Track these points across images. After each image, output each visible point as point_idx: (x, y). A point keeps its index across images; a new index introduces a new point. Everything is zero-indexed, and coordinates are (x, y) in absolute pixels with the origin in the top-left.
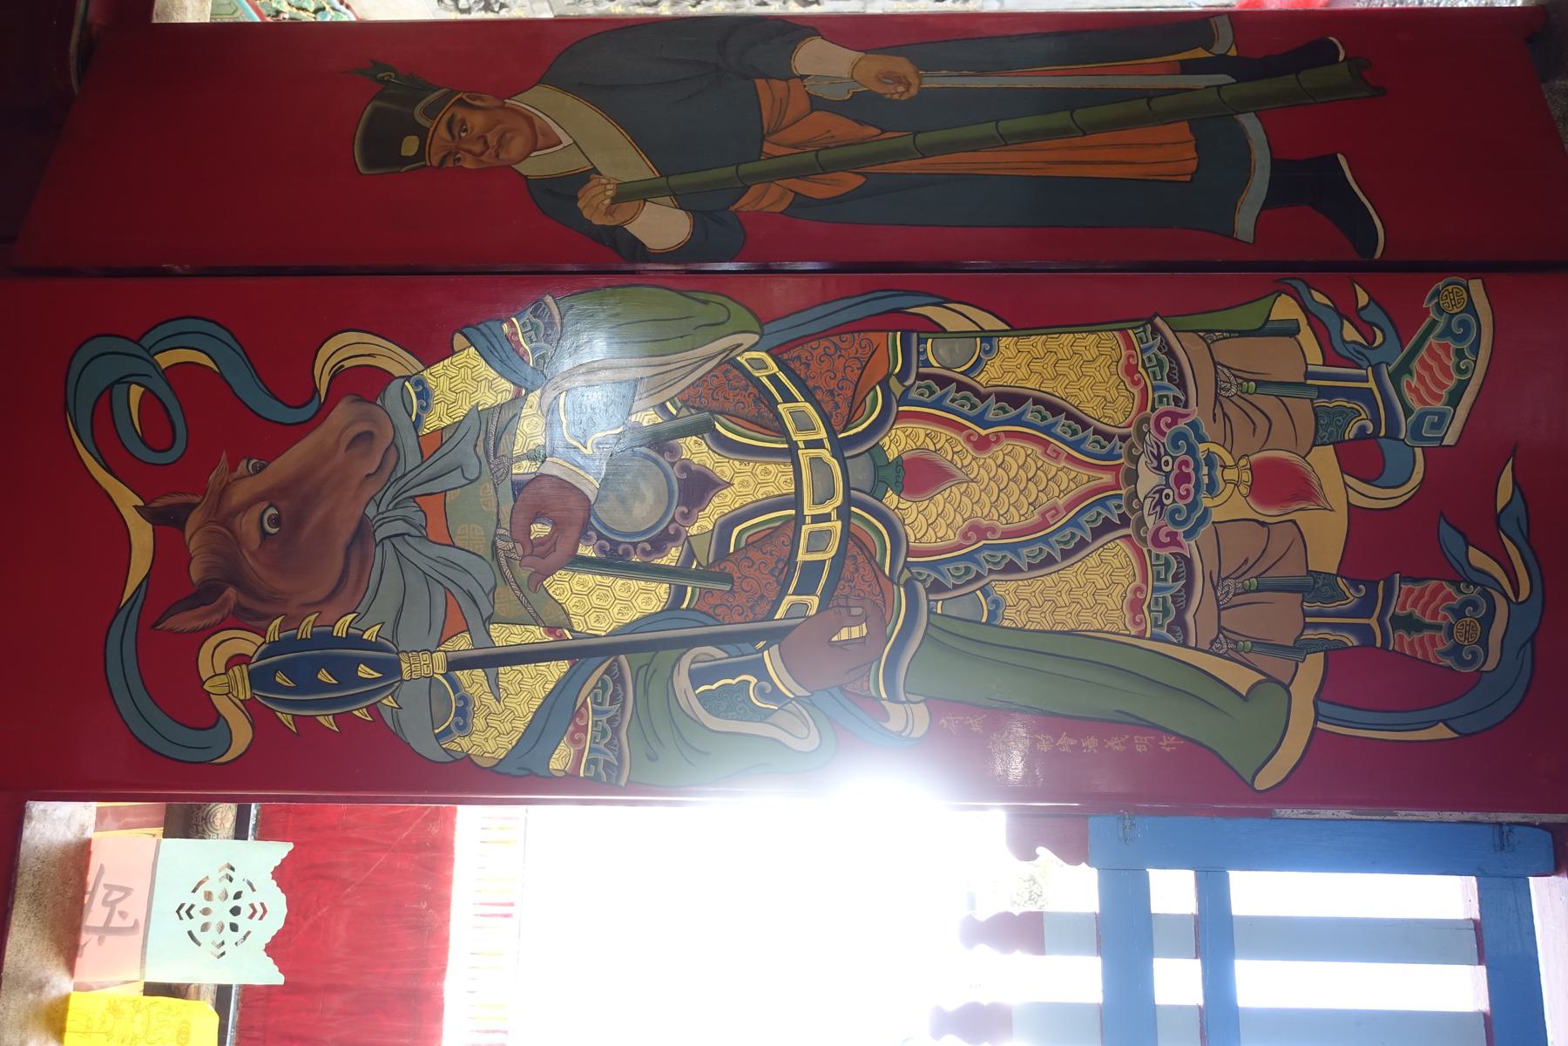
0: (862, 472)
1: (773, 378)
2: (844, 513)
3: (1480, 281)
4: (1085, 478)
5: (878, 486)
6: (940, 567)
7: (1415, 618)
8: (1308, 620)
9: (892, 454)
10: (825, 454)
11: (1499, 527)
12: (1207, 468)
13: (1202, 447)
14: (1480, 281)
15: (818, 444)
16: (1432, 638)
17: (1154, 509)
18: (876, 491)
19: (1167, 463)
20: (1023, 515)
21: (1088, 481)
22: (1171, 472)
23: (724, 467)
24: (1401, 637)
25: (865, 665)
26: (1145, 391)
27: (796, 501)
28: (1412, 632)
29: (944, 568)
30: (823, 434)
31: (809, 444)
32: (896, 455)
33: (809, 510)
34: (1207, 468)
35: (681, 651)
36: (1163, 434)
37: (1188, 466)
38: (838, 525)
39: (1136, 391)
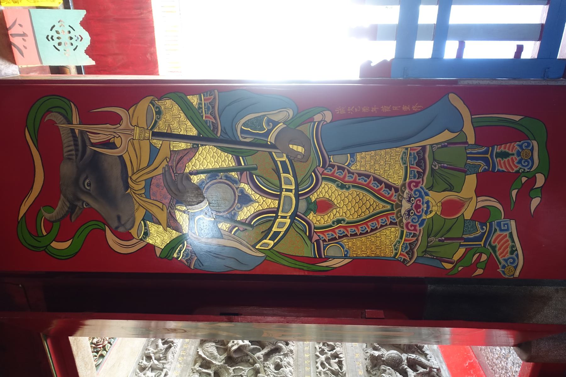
0: (303, 205)
1: (283, 163)
2: (292, 217)
3: (514, 221)
4: (382, 206)
5: (308, 210)
6: (325, 233)
7: (503, 151)
8: (468, 155)
9: (313, 199)
10: (292, 195)
11: (526, 117)
12: (426, 204)
13: (426, 197)
14: (514, 221)
15: (290, 191)
16: (512, 159)
17: (410, 194)
18: (307, 213)
19: (413, 200)
20: (359, 215)
21: (382, 208)
22: (414, 203)
23: (255, 196)
24: (500, 161)
25: (326, 108)
26: (396, 254)
27: (276, 212)
28: (504, 158)
29: (326, 234)
30: (293, 187)
31: (287, 190)
32: (314, 200)
33: (280, 214)
34: (426, 204)
35: (252, 142)
36: (411, 190)
37: (420, 202)
38: (289, 221)
39: (394, 252)
